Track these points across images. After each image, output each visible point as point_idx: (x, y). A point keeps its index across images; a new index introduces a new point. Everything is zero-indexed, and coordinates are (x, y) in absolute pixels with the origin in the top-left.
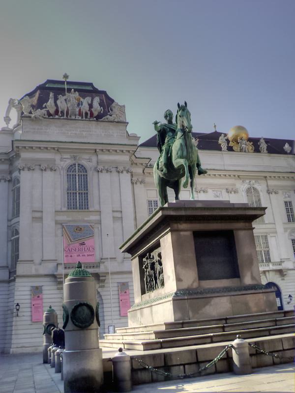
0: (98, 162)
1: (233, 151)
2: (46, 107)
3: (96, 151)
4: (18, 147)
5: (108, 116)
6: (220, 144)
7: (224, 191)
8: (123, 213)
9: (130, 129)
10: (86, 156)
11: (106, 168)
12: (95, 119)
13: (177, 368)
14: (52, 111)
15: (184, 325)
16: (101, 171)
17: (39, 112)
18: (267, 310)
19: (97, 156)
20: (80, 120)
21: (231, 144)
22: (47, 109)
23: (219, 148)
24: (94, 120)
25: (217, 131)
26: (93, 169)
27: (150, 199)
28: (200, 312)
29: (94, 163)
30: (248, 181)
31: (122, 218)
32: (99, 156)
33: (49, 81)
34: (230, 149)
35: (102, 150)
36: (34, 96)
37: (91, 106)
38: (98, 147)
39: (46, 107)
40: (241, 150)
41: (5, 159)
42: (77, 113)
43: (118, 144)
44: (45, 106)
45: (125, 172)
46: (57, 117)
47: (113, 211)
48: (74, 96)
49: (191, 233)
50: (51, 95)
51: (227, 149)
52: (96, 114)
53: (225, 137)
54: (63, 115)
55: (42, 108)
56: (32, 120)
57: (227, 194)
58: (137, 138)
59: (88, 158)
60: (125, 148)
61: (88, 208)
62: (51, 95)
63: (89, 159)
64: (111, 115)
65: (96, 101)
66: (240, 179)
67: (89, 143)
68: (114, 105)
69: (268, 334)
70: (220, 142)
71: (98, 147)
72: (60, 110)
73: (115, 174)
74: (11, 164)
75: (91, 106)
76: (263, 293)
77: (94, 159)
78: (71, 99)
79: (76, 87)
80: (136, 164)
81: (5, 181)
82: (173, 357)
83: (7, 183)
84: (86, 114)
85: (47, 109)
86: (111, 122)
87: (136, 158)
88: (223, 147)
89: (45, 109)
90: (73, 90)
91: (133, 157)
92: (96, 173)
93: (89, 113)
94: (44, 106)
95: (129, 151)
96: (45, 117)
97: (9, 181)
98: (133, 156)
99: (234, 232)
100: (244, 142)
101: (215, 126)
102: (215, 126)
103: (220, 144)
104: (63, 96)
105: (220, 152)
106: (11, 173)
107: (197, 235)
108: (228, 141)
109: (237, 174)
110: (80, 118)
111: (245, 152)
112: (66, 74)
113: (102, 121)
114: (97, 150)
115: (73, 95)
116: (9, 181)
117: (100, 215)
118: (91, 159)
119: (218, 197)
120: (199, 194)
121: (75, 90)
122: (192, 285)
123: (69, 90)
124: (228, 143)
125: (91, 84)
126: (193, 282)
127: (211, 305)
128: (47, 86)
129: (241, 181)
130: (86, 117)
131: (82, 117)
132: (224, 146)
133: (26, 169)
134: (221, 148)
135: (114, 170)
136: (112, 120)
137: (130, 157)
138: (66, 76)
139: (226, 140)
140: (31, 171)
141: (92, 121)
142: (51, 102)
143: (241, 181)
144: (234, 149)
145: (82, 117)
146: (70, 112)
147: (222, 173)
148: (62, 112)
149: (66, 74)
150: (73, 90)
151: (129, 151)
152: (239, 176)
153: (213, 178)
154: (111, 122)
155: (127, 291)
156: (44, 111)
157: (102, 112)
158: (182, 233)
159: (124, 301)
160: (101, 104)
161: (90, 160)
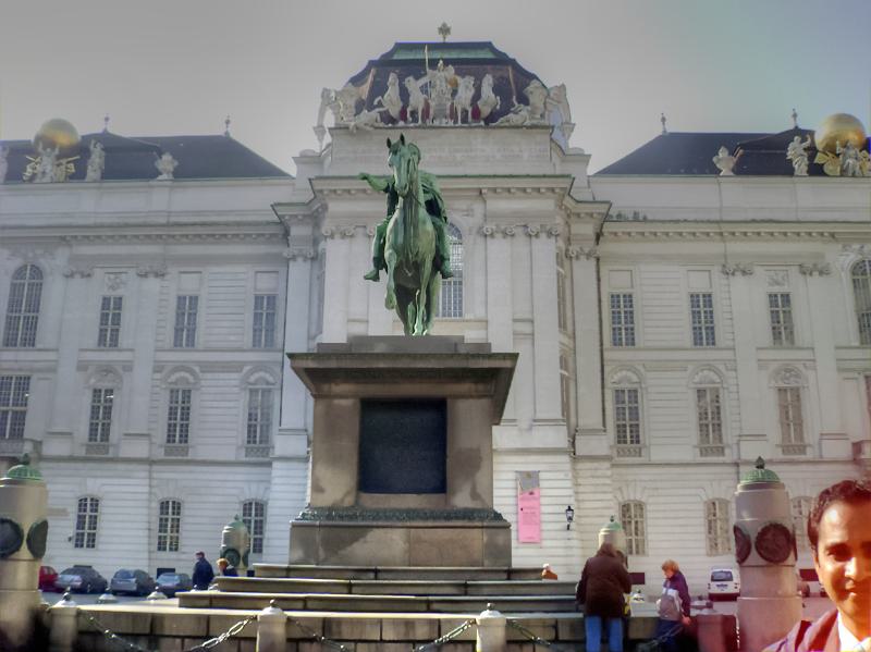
0: (485, 216)
1: (825, 175)
2: (380, 105)
3: (481, 193)
4: (321, 191)
5: (510, 115)
6: (791, 161)
7: (794, 271)
8: (536, 324)
9: (575, 142)
10: (463, 204)
11: (503, 227)
12: (482, 123)
13: (169, 640)
14: (394, 112)
15: (292, 574)
16: (492, 235)
17: (366, 116)
18: (486, 562)
19: (485, 202)
20: (451, 127)
21: (819, 159)
22: (381, 109)
23: (787, 170)
24: (481, 126)
25: (802, 127)
26: (475, 230)
27: (616, 292)
28: (342, 552)
29: (477, 219)
30: (856, 246)
31: (533, 334)
32: (488, 202)
33: (400, 47)
34: (816, 170)
35: (495, 190)
36: (366, 81)
37: (477, 96)
38: (485, 184)
39: (380, 105)
40: (843, 173)
41: (304, 216)
42: (448, 112)
43: (528, 176)
44: (380, 102)
45: (543, 236)
46: (401, 123)
47: (515, 321)
48: (442, 76)
49: (358, 401)
50: (392, 78)
51: (808, 172)
52: (485, 111)
53: (802, 142)
54: (415, 120)
55: (371, 108)
56: (352, 134)
57: (801, 277)
58: (584, 158)
59: (464, 207)
60: (544, 184)
61: (461, 315)
62: (392, 78)
63: (467, 211)
64: (517, 113)
65: (488, 82)
66: (837, 241)
67: (466, 176)
68: (533, 86)
69: (574, 608)
70: (790, 154)
71: (485, 184)
72: (409, 110)
73: (521, 240)
74: (317, 226)
75: (477, 96)
76: (482, 527)
77: (478, 208)
78: (438, 82)
79: (454, 55)
80: (578, 215)
81: (305, 258)
82: (167, 623)
83: (309, 261)
84: (465, 112)
85: (381, 109)
86: (517, 127)
87: (578, 202)
88: (796, 167)
89: (377, 110)
90: (441, 62)
91: (568, 202)
92: (480, 240)
93: (470, 110)
94: (375, 103)
95: (553, 190)
96: (376, 125)
97: (313, 259)
98: (567, 198)
99: (449, 401)
100: (852, 152)
101: (795, 116)
102: (795, 116)
103: (791, 161)
104: (417, 78)
105: (788, 179)
106: (315, 242)
107: (368, 405)
108: (812, 151)
109: (827, 229)
110: (451, 123)
111: (854, 175)
112: (444, 25)
113: (494, 128)
114: (483, 191)
115: (442, 74)
116: (313, 259)
117: (487, 329)
118: (472, 210)
119: (778, 283)
120: (731, 277)
121: (447, 62)
122: (342, 500)
123: (433, 63)
124: (811, 158)
125: (488, 46)
126: (348, 493)
127: (365, 542)
128: (396, 57)
129: (840, 246)
130: (464, 120)
131: (456, 122)
132: (801, 165)
133: (337, 236)
134: (793, 169)
135: (520, 231)
136: (519, 123)
137: (560, 205)
138: (445, 30)
139: (805, 149)
140: (348, 240)
141: (475, 127)
142: (392, 93)
143: (840, 246)
144: (827, 169)
145: (456, 122)
146: (431, 112)
147: (790, 229)
148: (414, 113)
149: (444, 25)
150: (441, 62)
151: (553, 190)
152: (832, 235)
153: (767, 241)
154: (517, 127)
155: (536, 491)
156: (375, 113)
157: (498, 107)
158: (336, 402)
159: (529, 511)
160: (496, 90)
161: (469, 213)
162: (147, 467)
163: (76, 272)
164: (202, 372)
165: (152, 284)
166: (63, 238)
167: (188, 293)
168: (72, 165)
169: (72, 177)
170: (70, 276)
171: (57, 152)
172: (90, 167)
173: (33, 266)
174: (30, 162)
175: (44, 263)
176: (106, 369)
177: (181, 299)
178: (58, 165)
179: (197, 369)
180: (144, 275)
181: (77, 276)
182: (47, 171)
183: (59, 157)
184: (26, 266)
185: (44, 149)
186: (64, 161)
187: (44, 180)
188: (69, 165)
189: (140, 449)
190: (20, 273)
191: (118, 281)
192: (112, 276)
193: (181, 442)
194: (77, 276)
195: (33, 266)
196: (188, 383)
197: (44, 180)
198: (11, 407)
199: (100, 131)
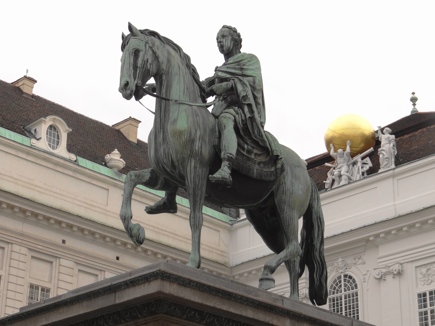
163: (386, 274)
166: (367, 240)
168: (368, 159)
169: (373, 171)
170: (381, 279)
171: (348, 149)
172: (381, 156)
173: (346, 276)
174: (330, 168)
178: (354, 163)
181: (389, 278)
182: (342, 173)
183: (353, 155)
184: (340, 277)
185: (335, 151)
186: (358, 158)
187: (342, 183)
188: (364, 161)
192: (424, 270)
194: (389, 278)
197: (342, 183)
199: (408, 114)
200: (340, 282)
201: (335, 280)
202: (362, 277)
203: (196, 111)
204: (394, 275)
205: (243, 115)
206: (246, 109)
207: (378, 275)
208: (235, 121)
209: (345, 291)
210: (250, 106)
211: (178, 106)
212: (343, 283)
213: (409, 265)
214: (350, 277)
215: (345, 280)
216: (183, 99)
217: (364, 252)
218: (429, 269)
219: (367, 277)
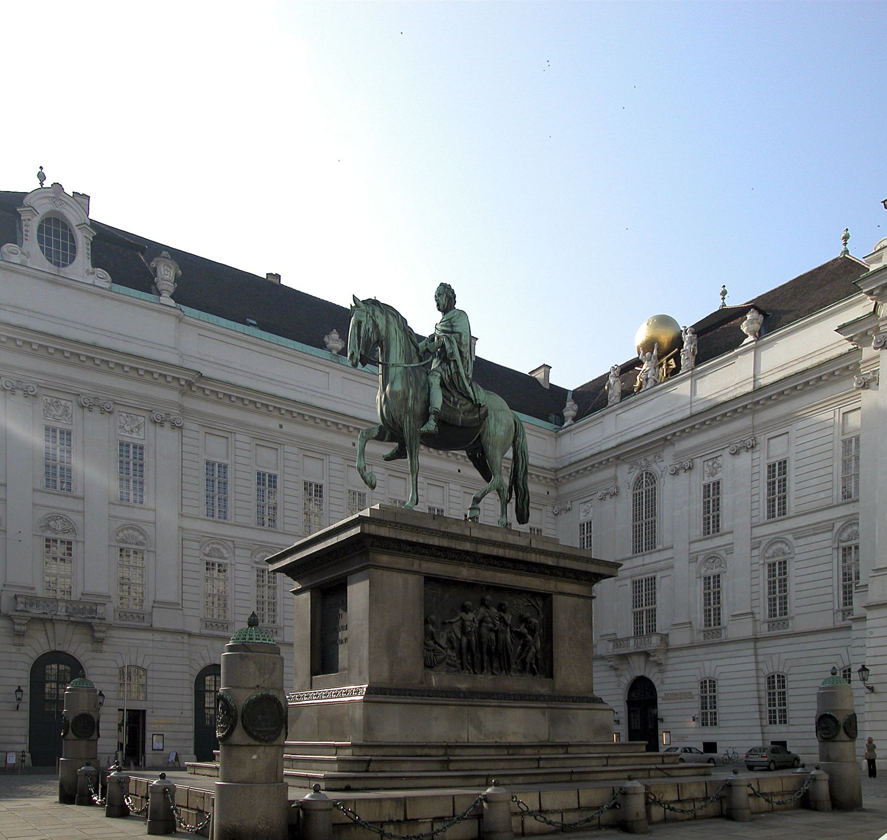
162: (752, 645)
164: (795, 539)
165: (745, 458)
167: (775, 460)
170: (676, 473)
175: (655, 468)
176: (713, 557)
177: (771, 467)
179: (790, 537)
180: (736, 453)
189: (745, 629)
190: (638, 483)
191: (715, 465)
192: (710, 463)
193: (781, 615)
195: (646, 473)
196: (784, 553)
198: (644, 608)
200: (642, 479)
201: (638, 478)
202: (660, 473)
203: (409, 371)
204: (686, 470)
205: (449, 371)
206: (452, 365)
207: (673, 471)
208: (441, 377)
209: (646, 486)
210: (455, 361)
211: (394, 368)
212: (644, 480)
213: (699, 459)
214: (651, 474)
215: (646, 477)
216: (398, 362)
217: (663, 450)
218: (715, 462)
219: (664, 472)
